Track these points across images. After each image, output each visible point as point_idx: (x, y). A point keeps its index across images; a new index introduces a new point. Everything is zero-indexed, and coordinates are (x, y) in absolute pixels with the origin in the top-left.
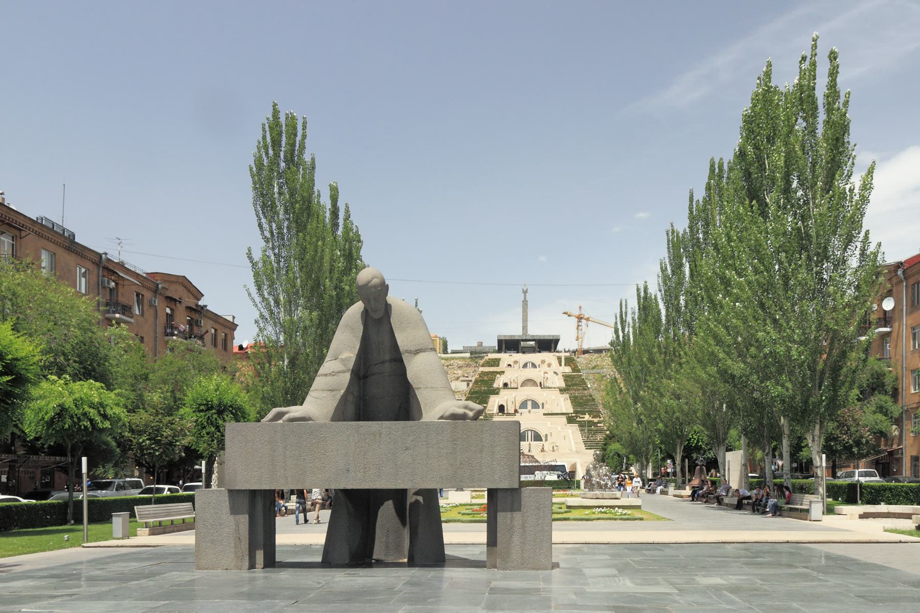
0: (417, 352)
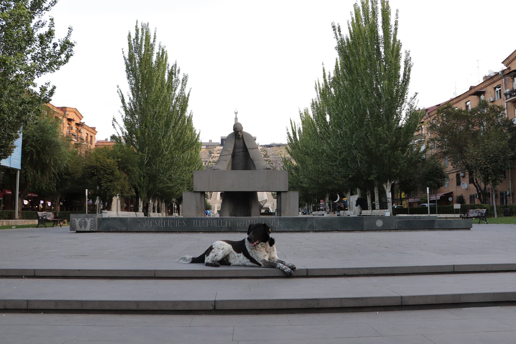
0: (253, 149)
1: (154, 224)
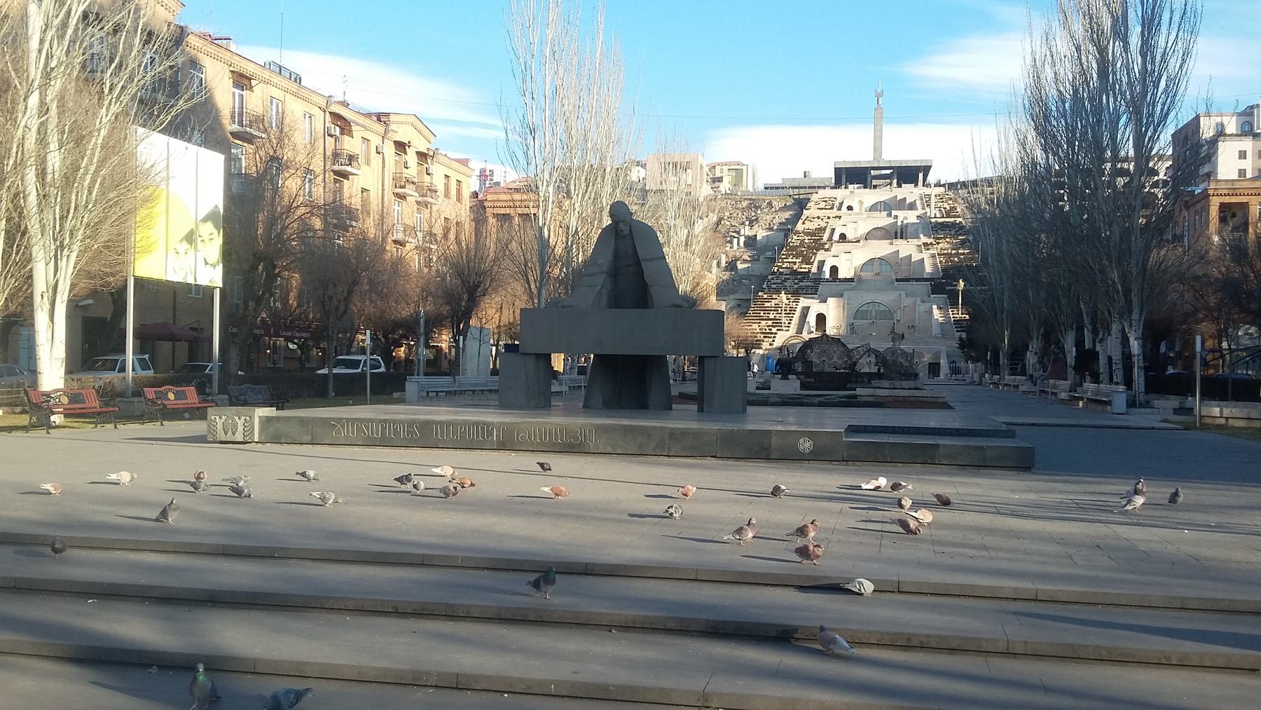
0: (651, 260)
1: (360, 430)
